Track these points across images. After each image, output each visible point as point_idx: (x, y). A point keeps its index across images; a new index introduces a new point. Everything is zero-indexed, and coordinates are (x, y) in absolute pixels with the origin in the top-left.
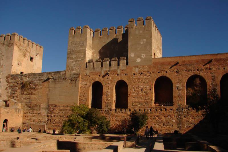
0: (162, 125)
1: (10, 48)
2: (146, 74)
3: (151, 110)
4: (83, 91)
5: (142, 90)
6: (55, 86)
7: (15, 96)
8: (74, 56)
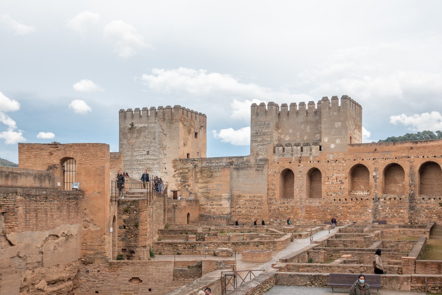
0: (358, 215)
1: (174, 126)
2: (341, 162)
3: (346, 199)
4: (272, 180)
5: (337, 179)
6: (238, 173)
7: (187, 185)
8: (259, 139)
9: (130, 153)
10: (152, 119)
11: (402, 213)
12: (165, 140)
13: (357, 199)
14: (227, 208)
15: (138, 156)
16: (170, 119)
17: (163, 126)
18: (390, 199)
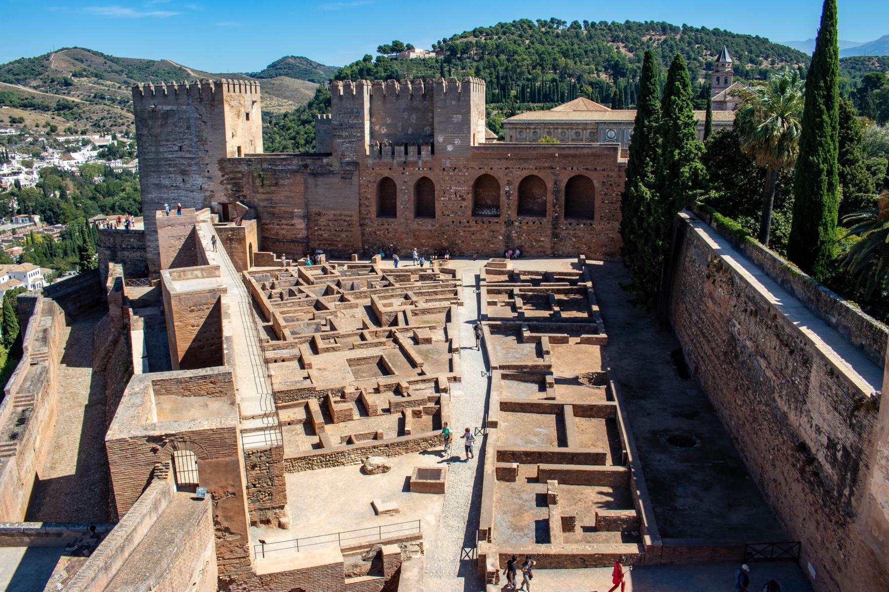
3: (468, 222)
8: (345, 134)
9: (153, 149)
10: (183, 99)
11: (543, 241)
13: (483, 222)
14: (301, 229)
18: (527, 223)
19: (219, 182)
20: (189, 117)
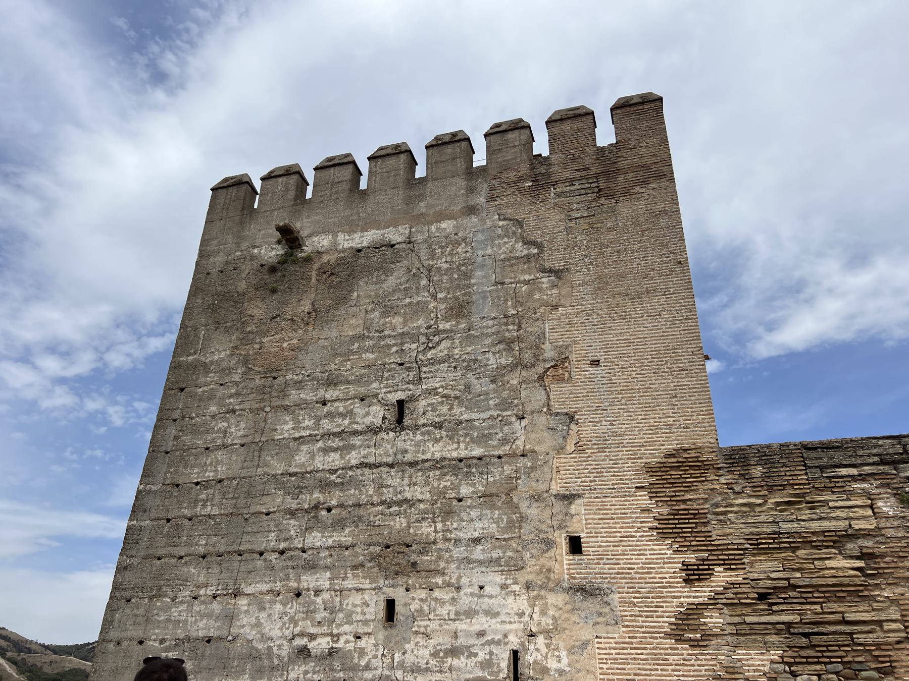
1: (625, 209)
12: (555, 307)
15: (304, 448)
16: (594, 170)
17: (531, 221)
19: (665, 622)
20: (469, 262)
